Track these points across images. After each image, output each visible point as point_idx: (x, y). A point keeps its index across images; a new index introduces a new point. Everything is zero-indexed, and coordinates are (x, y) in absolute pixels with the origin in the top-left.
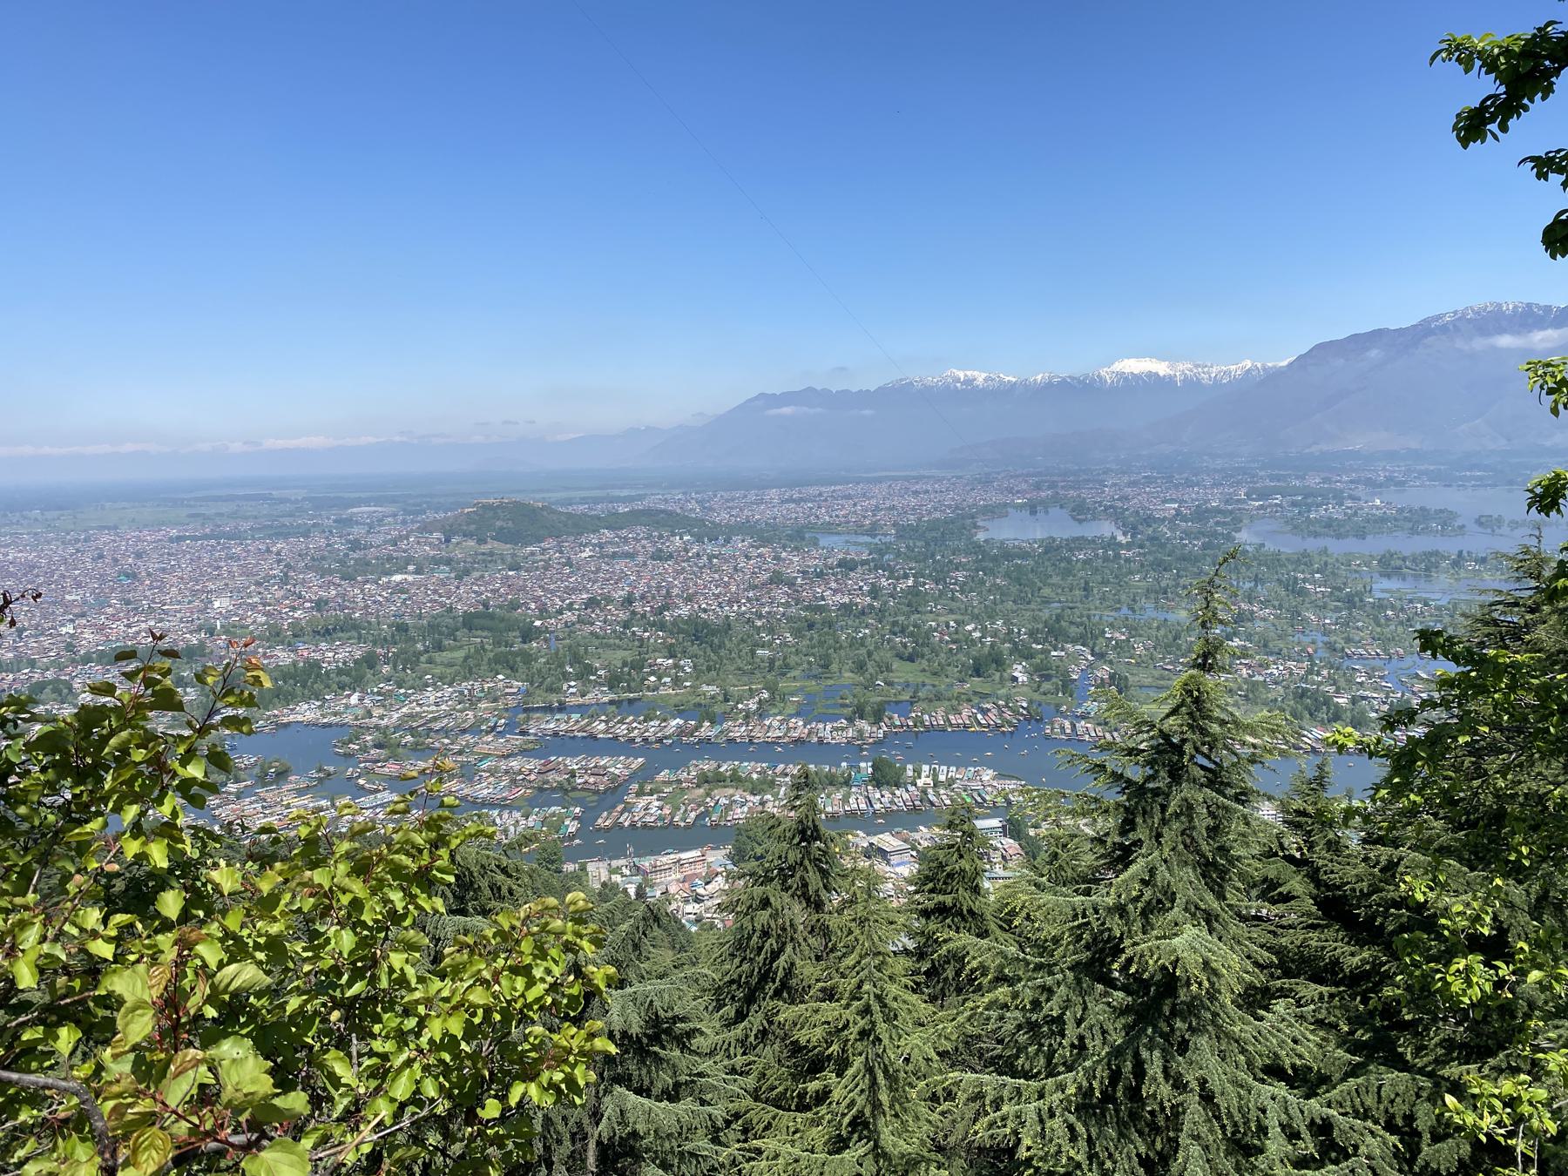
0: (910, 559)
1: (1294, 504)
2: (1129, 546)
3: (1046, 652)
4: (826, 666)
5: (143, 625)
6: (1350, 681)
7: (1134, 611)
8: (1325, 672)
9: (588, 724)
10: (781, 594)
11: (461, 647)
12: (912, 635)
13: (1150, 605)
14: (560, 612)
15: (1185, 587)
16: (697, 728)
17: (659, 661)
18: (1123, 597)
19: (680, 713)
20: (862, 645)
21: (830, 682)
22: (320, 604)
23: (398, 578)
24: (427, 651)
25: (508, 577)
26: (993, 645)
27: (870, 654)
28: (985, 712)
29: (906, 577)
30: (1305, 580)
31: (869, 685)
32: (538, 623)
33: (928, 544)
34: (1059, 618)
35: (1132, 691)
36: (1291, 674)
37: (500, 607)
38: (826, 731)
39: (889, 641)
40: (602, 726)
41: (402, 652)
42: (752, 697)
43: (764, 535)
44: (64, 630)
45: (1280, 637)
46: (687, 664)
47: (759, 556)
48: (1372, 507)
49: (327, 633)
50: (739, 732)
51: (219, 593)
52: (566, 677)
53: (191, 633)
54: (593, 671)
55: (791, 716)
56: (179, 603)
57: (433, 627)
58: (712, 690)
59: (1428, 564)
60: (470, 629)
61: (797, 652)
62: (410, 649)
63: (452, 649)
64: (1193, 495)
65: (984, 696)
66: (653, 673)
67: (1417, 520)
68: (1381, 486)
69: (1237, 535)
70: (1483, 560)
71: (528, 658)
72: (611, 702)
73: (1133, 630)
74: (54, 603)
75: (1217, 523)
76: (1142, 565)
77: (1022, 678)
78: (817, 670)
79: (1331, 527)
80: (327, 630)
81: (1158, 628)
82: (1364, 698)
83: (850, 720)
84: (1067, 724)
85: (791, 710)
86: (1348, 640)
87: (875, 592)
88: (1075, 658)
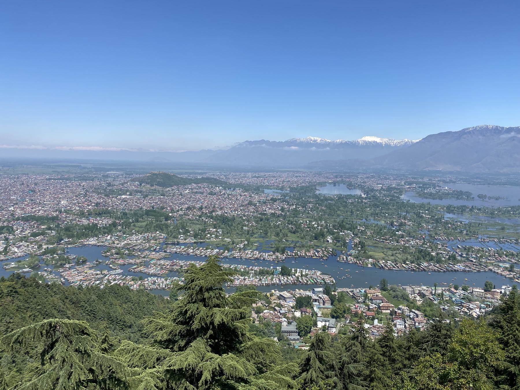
0: (294, 199)
1: (419, 187)
2: (366, 198)
3: (338, 233)
4: (266, 234)
5: (37, 208)
6: (436, 247)
7: (367, 220)
8: (428, 244)
9: (187, 250)
10: (252, 208)
11: (144, 221)
12: (294, 225)
13: (372, 219)
14: (178, 211)
15: (383, 213)
16: (223, 253)
17: (211, 229)
18: (364, 216)
19: (218, 248)
20: (278, 227)
21: (267, 239)
22: (97, 204)
23: (123, 197)
24: (133, 222)
25: (160, 198)
26: (321, 229)
27: (281, 230)
28: (318, 252)
29: (293, 205)
30: (422, 213)
31: (280, 241)
32: (170, 214)
33: (300, 194)
34: (343, 221)
35: (366, 247)
36: (417, 244)
37: (158, 208)
38: (266, 255)
39: (287, 226)
40: (192, 251)
41: (125, 222)
42: (241, 243)
43: (246, 188)
44: (10, 209)
45: (414, 232)
46: (220, 231)
47: (245, 195)
48: (445, 190)
49: (100, 214)
50: (237, 255)
51: (63, 199)
52: (180, 233)
53: (53, 212)
54: (189, 232)
55: (255, 250)
56: (50, 201)
57: (135, 214)
58: (228, 240)
59: (462, 210)
60: (148, 215)
61: (257, 229)
62: (127, 221)
63: (141, 222)
64: (387, 183)
65: (318, 247)
66: (209, 233)
67: (459, 195)
68: (447, 183)
69: (401, 197)
70: (479, 209)
71: (167, 226)
72: (195, 243)
73: (367, 227)
74: (7, 199)
75: (395, 192)
76: (370, 205)
77: (330, 241)
78: (263, 235)
79: (431, 196)
80: (100, 213)
81: (375, 227)
82: (441, 253)
83: (274, 252)
84: (345, 257)
85: (254, 248)
86: (436, 234)
87: (283, 210)
88: (348, 235)
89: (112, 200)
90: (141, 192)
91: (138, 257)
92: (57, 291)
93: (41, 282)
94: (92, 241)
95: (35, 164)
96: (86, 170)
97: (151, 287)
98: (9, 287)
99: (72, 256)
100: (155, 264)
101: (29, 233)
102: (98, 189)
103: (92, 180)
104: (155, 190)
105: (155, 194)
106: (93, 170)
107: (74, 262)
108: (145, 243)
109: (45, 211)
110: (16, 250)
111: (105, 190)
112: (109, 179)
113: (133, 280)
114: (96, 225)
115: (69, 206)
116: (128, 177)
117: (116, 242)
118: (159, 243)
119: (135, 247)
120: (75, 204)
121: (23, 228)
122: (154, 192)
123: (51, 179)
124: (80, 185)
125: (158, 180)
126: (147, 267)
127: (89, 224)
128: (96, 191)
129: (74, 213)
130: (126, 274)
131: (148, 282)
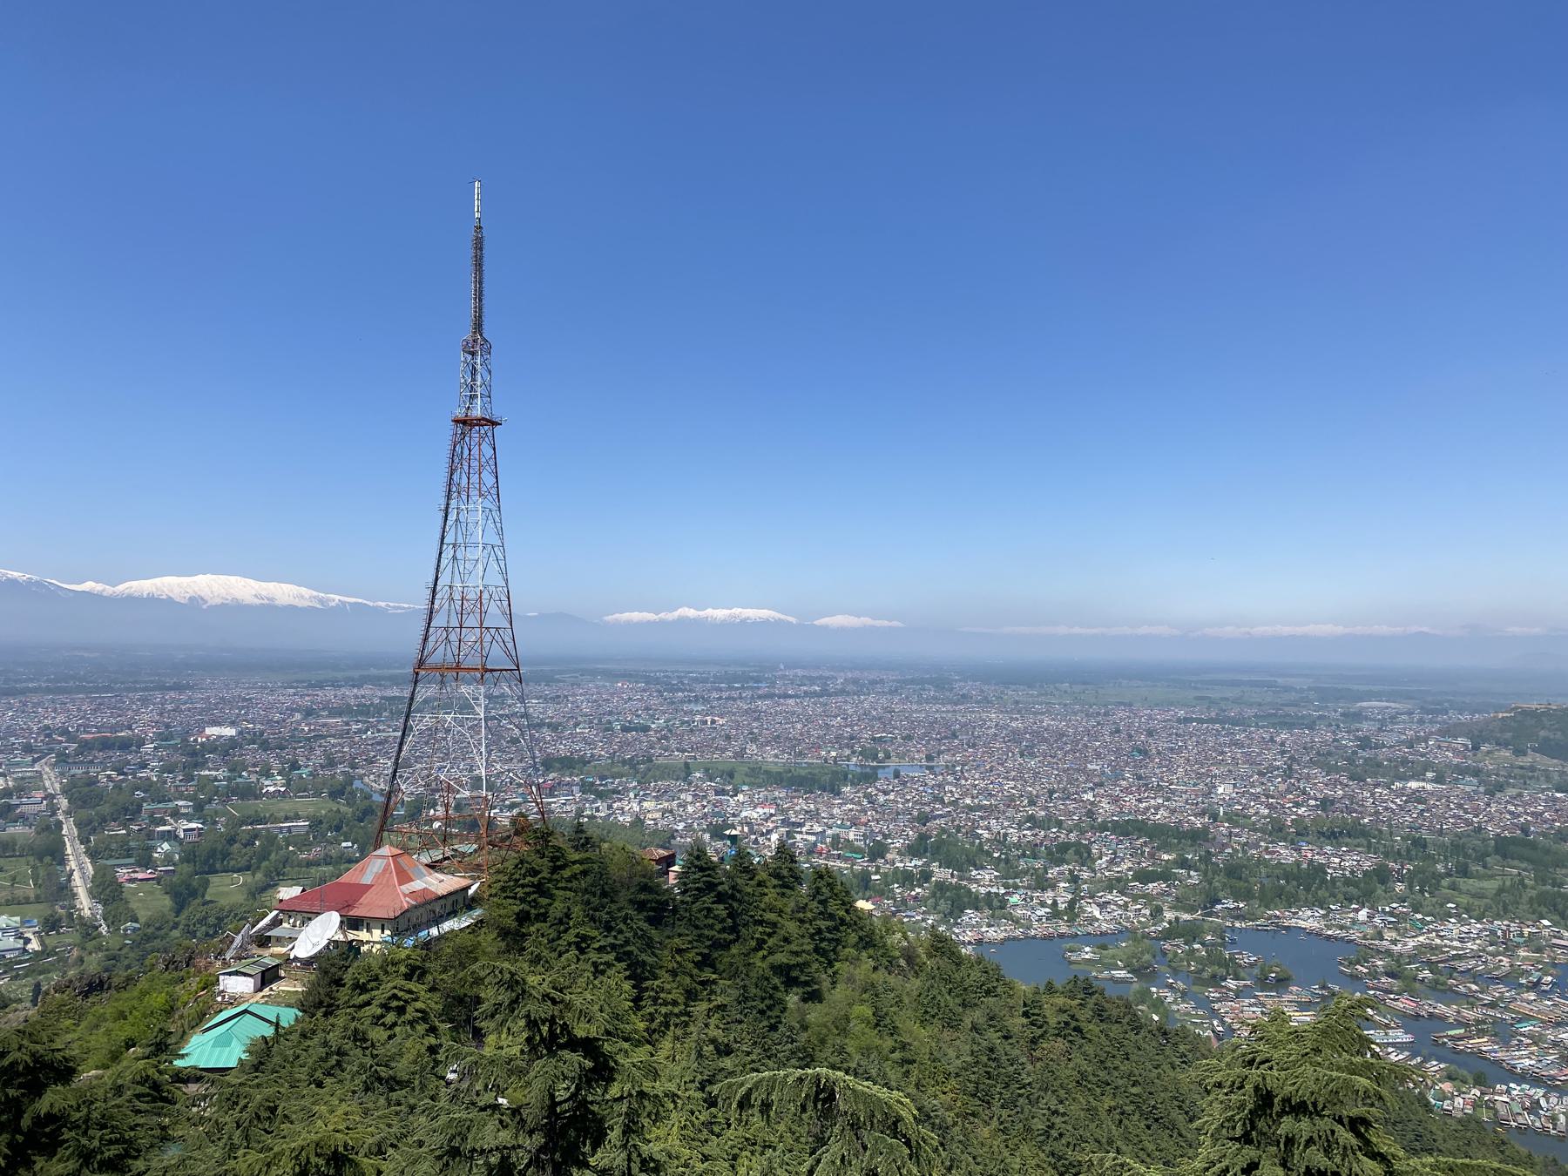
11: (1491, 877)
22: (1326, 803)
23: (1413, 785)
25: (1555, 800)
37: (1544, 835)
41: (1418, 870)
44: (1085, 797)
53: (1195, 815)
56: (1185, 784)
57: (1457, 848)
60: (1505, 857)
62: (1430, 868)
63: (1480, 877)
74: (1078, 770)
80: (1333, 833)
89: (1373, 794)
90: (1476, 773)
91: (1471, 1000)
92: (1190, 1056)
93: (1156, 1018)
94: (1308, 919)
95: (1149, 675)
96: (1293, 696)
97: (1520, 1120)
98: (1062, 1011)
99: (1247, 958)
100: (1536, 1040)
101: (1130, 869)
102: (1329, 754)
103: (1311, 728)
104: (1532, 769)
105: (1531, 782)
106: (1312, 695)
107: (1251, 977)
108: (1494, 955)
109: (1173, 811)
110: (1097, 913)
111: (1351, 760)
112: (1365, 726)
113: (1450, 1078)
114: (1321, 869)
115: (1239, 803)
116: (1431, 722)
117: (1389, 935)
118: (1554, 965)
119: (1456, 964)
120: (1256, 797)
121: (1115, 853)
122: (1527, 776)
123: (1191, 720)
124: (1272, 740)
125: (1542, 733)
126: (1506, 1044)
127: (1298, 864)
128: (1323, 760)
129: (1254, 824)
130: (1425, 1052)
131: (1508, 1097)
